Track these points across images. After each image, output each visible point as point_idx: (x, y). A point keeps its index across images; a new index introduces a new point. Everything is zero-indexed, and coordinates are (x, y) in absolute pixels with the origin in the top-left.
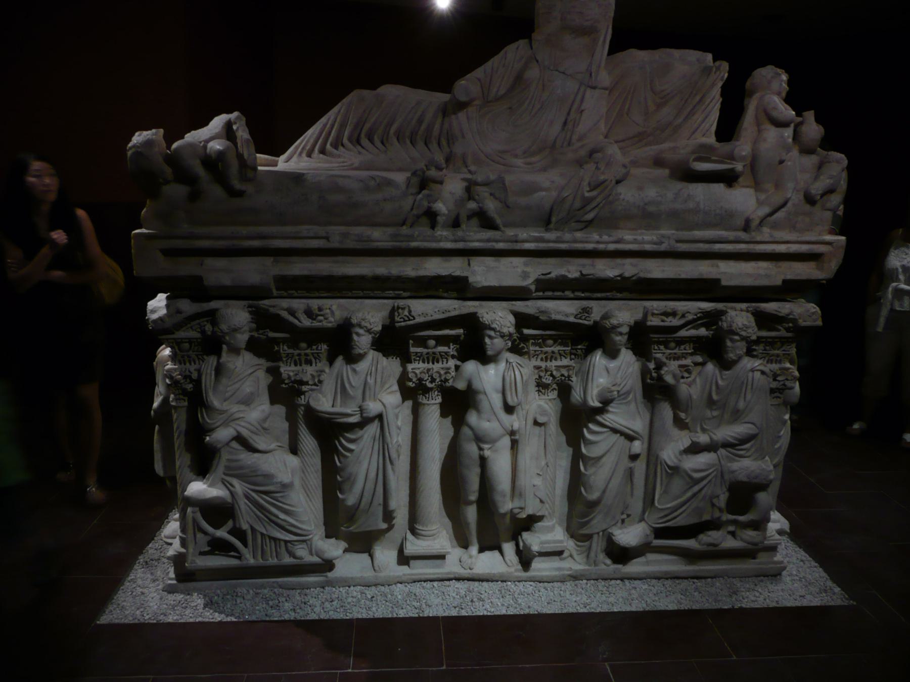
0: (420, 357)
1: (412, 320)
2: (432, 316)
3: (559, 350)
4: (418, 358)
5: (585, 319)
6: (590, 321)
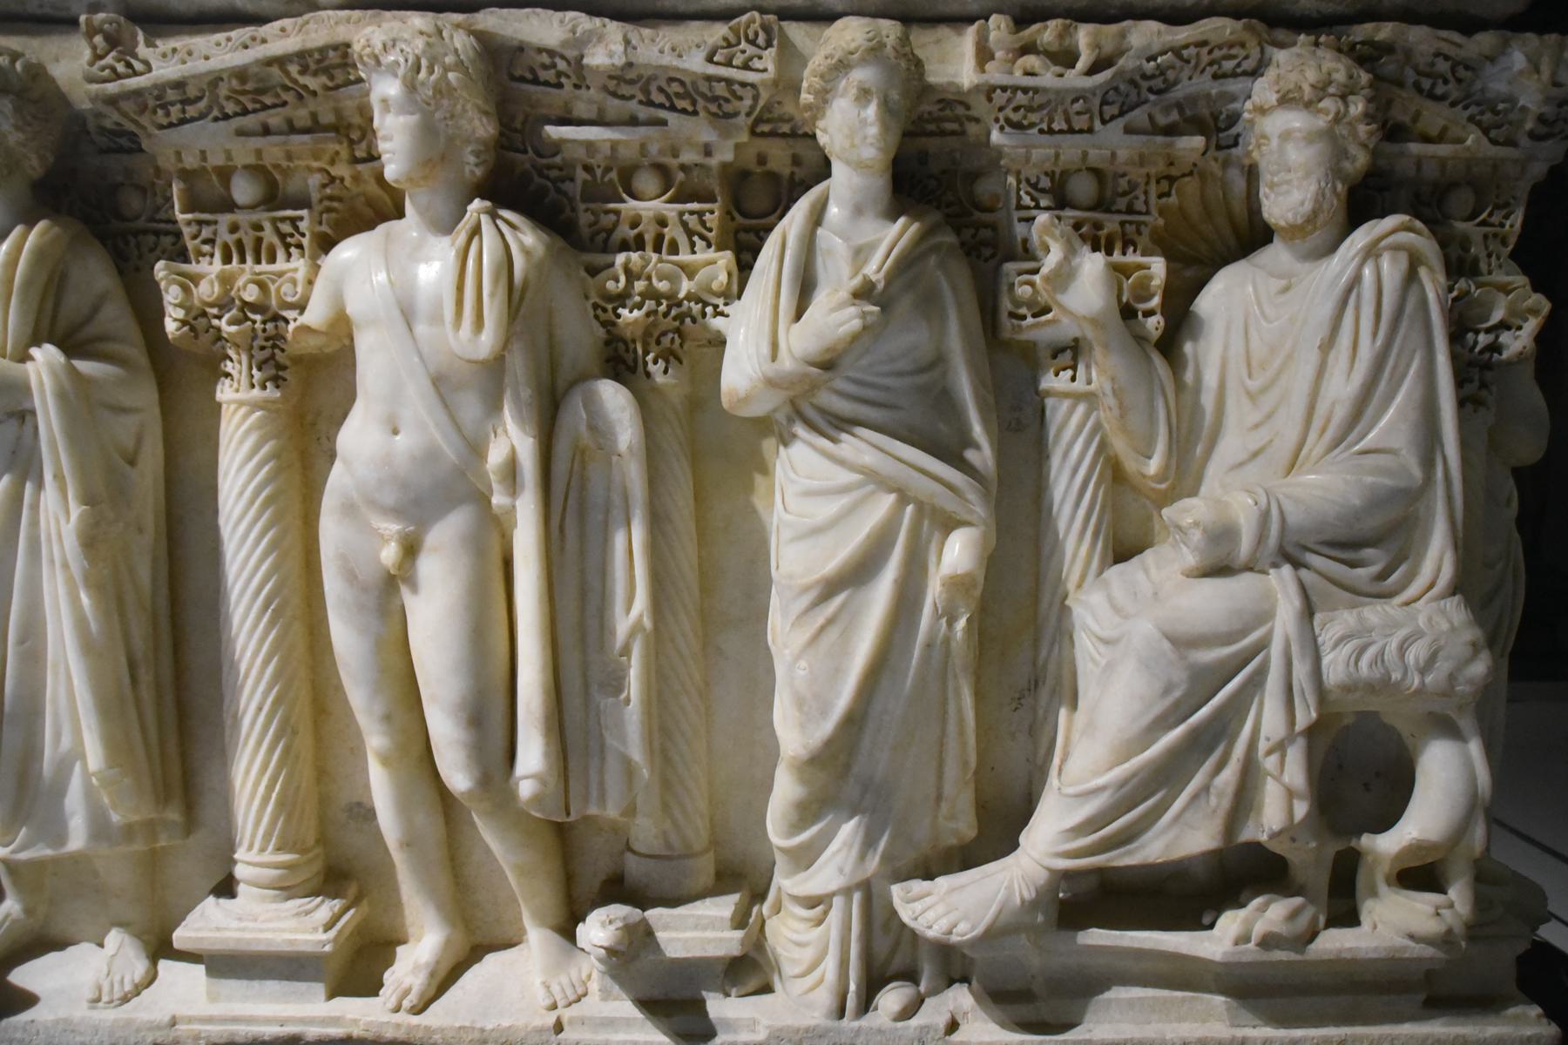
0: (210, 242)
1: (141, 74)
2: (207, 58)
3: (681, 214)
4: (206, 248)
5: (746, 67)
6: (765, 70)
